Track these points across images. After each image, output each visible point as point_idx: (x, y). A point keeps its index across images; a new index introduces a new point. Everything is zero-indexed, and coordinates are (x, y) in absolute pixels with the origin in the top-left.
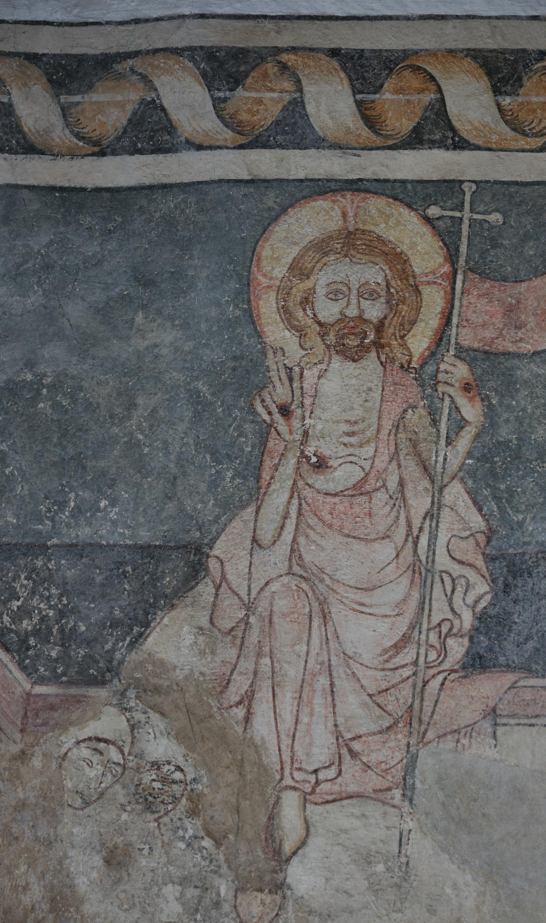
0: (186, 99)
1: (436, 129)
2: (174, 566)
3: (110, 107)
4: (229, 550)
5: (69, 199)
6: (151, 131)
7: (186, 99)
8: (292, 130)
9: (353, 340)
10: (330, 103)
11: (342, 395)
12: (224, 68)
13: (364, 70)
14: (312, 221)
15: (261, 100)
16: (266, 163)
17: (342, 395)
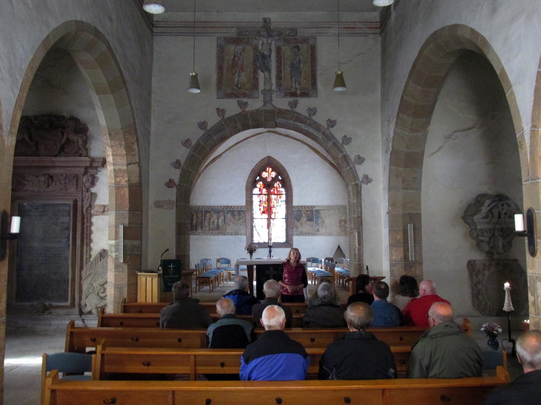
2: (300, 219)
17: (304, 215)
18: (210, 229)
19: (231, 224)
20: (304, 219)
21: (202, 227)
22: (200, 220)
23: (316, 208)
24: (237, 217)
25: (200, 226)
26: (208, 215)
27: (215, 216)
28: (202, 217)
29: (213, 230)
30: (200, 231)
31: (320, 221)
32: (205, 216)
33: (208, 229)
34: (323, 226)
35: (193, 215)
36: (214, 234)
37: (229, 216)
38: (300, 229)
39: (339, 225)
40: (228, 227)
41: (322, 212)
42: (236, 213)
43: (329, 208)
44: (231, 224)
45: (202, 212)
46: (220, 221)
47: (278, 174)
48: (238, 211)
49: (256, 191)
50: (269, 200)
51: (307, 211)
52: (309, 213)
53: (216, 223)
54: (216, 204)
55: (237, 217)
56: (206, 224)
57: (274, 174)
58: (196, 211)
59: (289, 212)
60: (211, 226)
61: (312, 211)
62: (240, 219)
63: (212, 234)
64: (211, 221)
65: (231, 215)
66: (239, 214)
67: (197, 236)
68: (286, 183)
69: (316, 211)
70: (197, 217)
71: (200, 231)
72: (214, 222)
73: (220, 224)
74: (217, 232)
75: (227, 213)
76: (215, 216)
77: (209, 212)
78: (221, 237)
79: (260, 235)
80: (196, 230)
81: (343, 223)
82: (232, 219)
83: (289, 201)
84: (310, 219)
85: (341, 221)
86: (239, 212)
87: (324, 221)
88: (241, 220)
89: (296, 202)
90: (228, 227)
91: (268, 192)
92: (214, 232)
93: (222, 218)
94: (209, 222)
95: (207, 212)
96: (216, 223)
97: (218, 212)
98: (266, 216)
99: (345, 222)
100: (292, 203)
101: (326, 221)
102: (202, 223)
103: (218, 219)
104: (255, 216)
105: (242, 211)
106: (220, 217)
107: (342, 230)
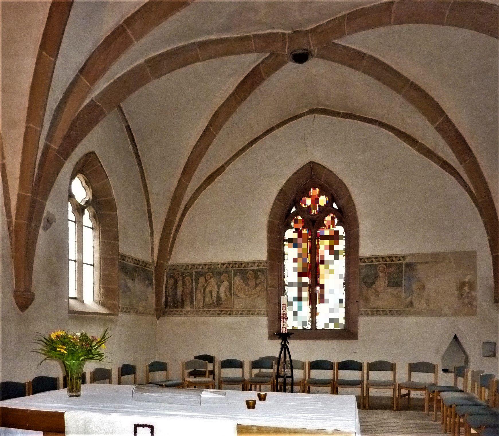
0: (374, 260)
1: (386, 261)
3: (370, 260)
4: (376, 282)
5: (368, 265)
6: (372, 261)
7: (374, 260)
8: (379, 261)
9: (382, 272)
10: (381, 260)
11: (381, 274)
12: (376, 258)
13: (382, 258)
14: (380, 266)
15: (377, 260)
16: (378, 263)
17: (381, 274)
18: (205, 305)
19: (241, 295)
20: (382, 283)
21: (192, 302)
22: (188, 290)
23: (408, 260)
24: (252, 283)
25: (188, 301)
26: (202, 279)
27: (213, 281)
28: (192, 284)
29: (210, 306)
30: (188, 308)
31: (414, 287)
32: (197, 283)
33: (201, 304)
34: (422, 297)
35: (176, 281)
36: (212, 314)
37: (238, 279)
38: (374, 303)
39: (456, 293)
40: (236, 300)
41: (419, 267)
42: (250, 275)
43: (435, 259)
44: (241, 295)
45: (191, 275)
46: (222, 289)
47: (332, 199)
48: (253, 270)
49: (289, 234)
50: (314, 250)
51: (389, 266)
52: (392, 270)
53: (215, 294)
54: (215, 261)
55: (252, 283)
56: (199, 296)
57: (323, 200)
58: (182, 273)
59: (352, 270)
60: (207, 300)
61: (399, 266)
62: (257, 285)
63: (208, 314)
64: (208, 290)
65: (242, 279)
66: (256, 277)
67: (183, 318)
68: (347, 216)
69: (408, 265)
70: (184, 284)
71: (188, 308)
72: (211, 292)
73: (222, 295)
74: (217, 309)
75: (234, 276)
76: (213, 281)
77: (204, 274)
78: (224, 319)
79: (297, 317)
80: (182, 307)
81: (466, 289)
82: (243, 285)
83: (351, 251)
84: (395, 283)
85: (461, 286)
86: (256, 272)
87: (423, 287)
88: (259, 288)
89: (366, 249)
90: (236, 300)
91: (310, 233)
92: (212, 310)
93: (226, 284)
94: (204, 292)
95: (199, 274)
96: (215, 294)
97: (220, 274)
98: (306, 280)
99: (472, 285)
100: (357, 252)
101: (428, 285)
102: (191, 294)
103: (219, 287)
104: (287, 280)
105: (261, 271)
106: (222, 282)
107: (463, 303)
